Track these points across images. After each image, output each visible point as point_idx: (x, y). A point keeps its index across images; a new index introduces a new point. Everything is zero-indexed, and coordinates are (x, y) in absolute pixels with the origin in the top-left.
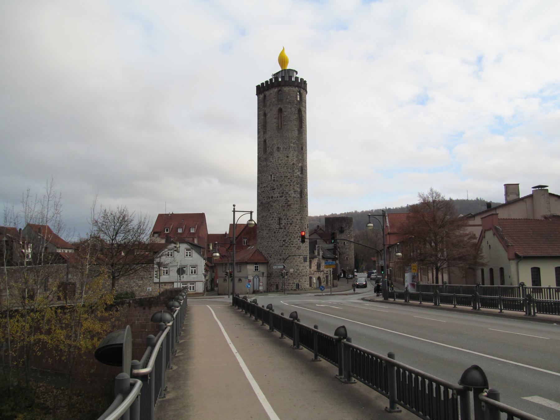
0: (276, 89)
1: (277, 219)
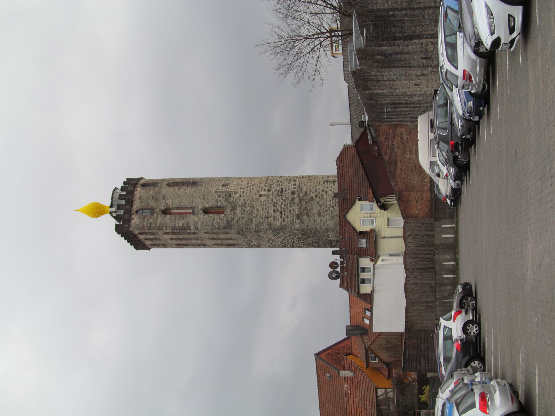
1: (326, 185)
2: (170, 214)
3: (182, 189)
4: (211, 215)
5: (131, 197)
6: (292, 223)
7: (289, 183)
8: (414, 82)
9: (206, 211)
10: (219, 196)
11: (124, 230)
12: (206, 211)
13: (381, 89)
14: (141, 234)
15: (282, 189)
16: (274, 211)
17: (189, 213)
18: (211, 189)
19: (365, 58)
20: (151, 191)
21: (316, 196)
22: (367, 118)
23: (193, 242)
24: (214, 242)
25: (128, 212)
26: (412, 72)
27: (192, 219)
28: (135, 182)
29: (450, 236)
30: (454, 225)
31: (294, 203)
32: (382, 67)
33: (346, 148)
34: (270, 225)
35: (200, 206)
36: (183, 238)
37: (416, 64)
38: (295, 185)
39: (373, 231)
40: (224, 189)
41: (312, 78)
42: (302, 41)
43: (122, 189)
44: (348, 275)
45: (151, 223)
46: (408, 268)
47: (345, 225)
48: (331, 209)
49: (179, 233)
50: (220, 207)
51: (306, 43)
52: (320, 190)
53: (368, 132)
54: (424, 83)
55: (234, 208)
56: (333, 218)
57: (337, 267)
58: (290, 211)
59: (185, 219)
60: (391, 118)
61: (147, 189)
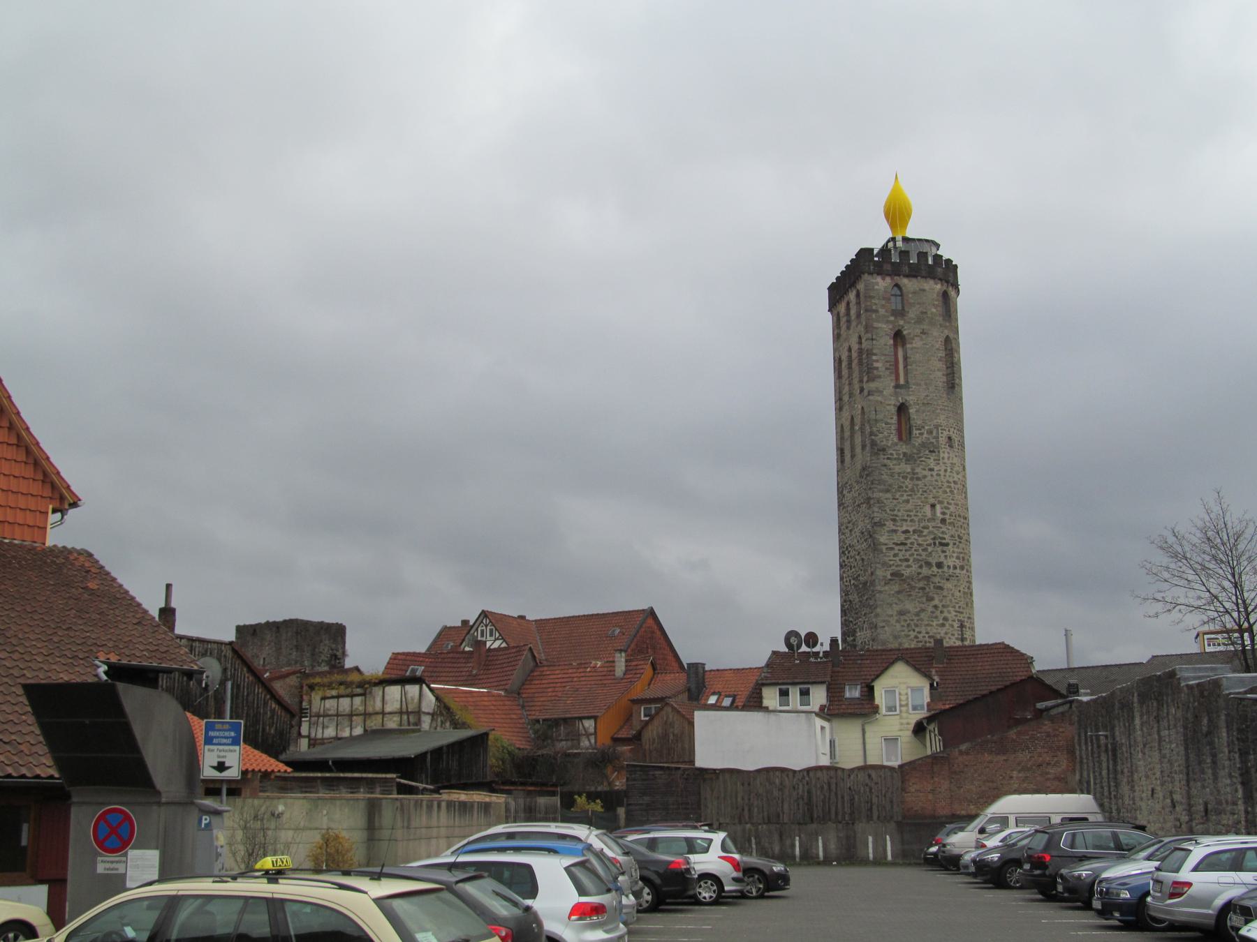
0: (939, 286)
1: (956, 625)
2: (895, 345)
3: (941, 365)
4: (895, 417)
5: (924, 273)
6: (884, 564)
7: (958, 558)
8: (1159, 788)
9: (902, 409)
10: (930, 432)
11: (863, 263)
12: (902, 409)
13: (1142, 725)
14: (858, 295)
15: (947, 545)
16: (906, 532)
17: (897, 378)
18: (942, 417)
19: (1202, 695)
20: (935, 311)
21: (936, 607)
22: (1085, 699)
23: (846, 388)
24: (847, 424)
25: (896, 271)
26: (1177, 783)
27: (885, 384)
28: (951, 279)
29: (871, 850)
30: (889, 858)
31: (921, 567)
32: (1185, 728)
33: (1027, 661)
34: (880, 524)
35: (911, 399)
36: (852, 369)
37: (1194, 792)
38: (955, 568)
39: (876, 709)
40: (943, 440)
41: (1159, 596)
42: (1230, 577)
43: (938, 258)
44: (794, 666)
45: (876, 311)
46: (811, 774)
47: (885, 659)
48: (912, 634)
49: (860, 363)
50: (910, 433)
51: (1226, 584)
52: (945, 614)
53: (1060, 701)
54: (1158, 807)
55: (908, 458)
56: (896, 637)
57: (808, 646)
58: (907, 560)
59: (888, 372)
60: (1086, 743)
61: (939, 302)
